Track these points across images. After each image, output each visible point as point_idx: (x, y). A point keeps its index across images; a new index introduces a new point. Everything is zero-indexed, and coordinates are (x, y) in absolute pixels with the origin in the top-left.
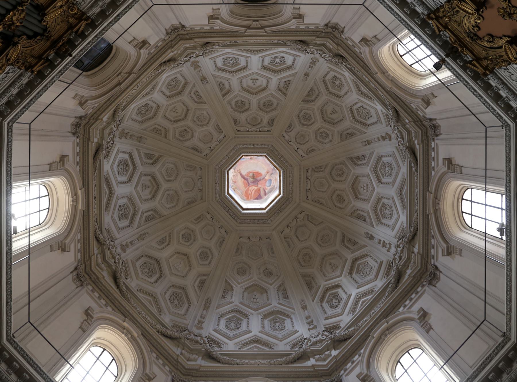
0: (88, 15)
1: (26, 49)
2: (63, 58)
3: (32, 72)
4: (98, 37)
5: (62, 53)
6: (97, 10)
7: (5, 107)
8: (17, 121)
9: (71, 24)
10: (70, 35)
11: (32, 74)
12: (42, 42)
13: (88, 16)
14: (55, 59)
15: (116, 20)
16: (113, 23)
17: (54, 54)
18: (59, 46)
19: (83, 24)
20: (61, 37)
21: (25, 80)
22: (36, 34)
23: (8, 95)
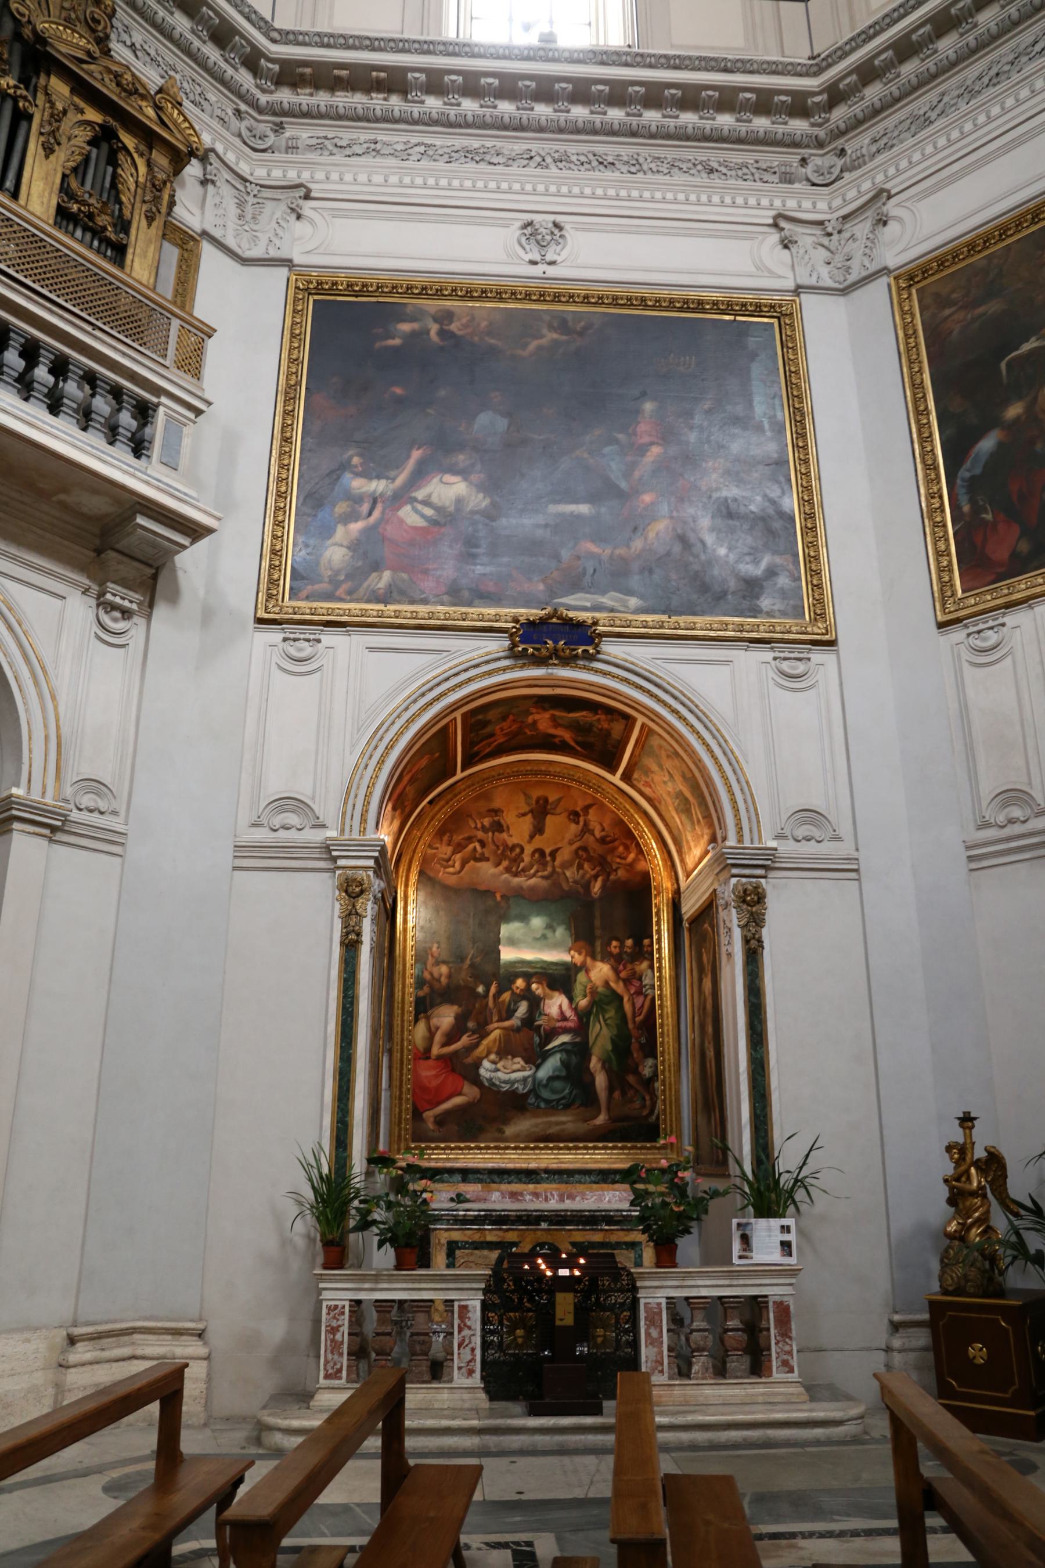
7: (231, 51)
8: (269, 18)
23: (197, 43)
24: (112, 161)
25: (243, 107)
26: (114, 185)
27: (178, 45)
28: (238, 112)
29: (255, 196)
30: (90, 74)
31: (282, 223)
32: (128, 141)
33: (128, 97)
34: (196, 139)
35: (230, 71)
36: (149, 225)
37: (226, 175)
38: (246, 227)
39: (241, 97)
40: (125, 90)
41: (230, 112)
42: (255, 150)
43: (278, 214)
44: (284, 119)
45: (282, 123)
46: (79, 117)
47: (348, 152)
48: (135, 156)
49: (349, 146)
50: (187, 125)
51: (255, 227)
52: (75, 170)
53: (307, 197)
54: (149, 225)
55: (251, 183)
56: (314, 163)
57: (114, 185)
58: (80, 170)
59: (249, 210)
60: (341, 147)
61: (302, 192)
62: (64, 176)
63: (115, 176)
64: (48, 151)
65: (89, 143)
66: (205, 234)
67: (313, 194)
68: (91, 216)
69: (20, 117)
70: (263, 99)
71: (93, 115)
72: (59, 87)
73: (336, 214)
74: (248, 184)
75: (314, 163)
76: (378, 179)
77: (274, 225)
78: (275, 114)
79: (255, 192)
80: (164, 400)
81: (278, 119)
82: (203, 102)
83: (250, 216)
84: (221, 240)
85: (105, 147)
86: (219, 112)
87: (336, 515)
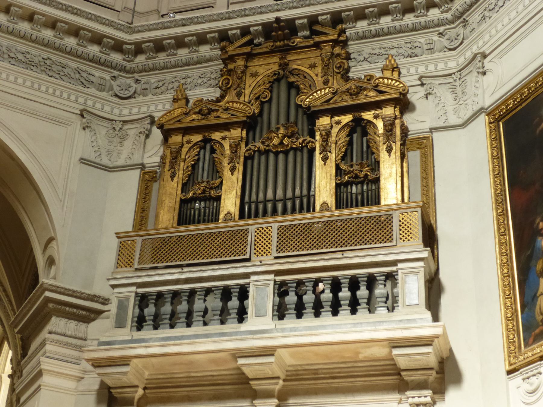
0: (220, 53)
1: (315, 78)
2: (291, 22)
3: (343, 31)
4: (227, 15)
5: (287, 31)
6: (205, 50)
7: (417, 10)
9: (247, 61)
10: (260, 44)
11: (345, 29)
12: (295, 66)
13: (221, 51)
14: (303, 27)
15: (189, 21)
16: (196, 20)
17: (299, 34)
18: (282, 42)
19: (231, 50)
20: (271, 52)
21: (362, 25)
22: (291, 86)
24: (365, 133)
25: (441, 29)
26: (368, 147)
27: (389, 33)
28: (441, 34)
29: (460, 79)
30: (336, 102)
31: (477, 85)
32: (368, 115)
33: (357, 97)
34: (401, 85)
35: (422, 20)
36: (390, 155)
37: (437, 81)
38: (461, 102)
39: (438, 25)
40: (354, 95)
41: (436, 38)
42: (454, 49)
43: (474, 79)
44: (464, 17)
45: (464, 19)
46: (340, 126)
47: (497, 9)
48: (374, 121)
49: (496, 5)
50: (394, 82)
51: (464, 99)
52: (343, 158)
53: (485, 56)
54: (390, 155)
55: (454, 73)
56: (482, 33)
57: (368, 147)
58: (345, 156)
59: (459, 90)
60: (493, 9)
61: (479, 57)
62: (338, 167)
63: (368, 141)
64: (325, 159)
65: (348, 136)
66: (432, 130)
67: (487, 52)
68: (357, 176)
69: (312, 152)
70: (449, 15)
71: (347, 119)
72: (324, 121)
73: (501, 56)
74: (453, 76)
75: (482, 33)
76: (513, 14)
77: (474, 88)
78: (459, 18)
79: (459, 77)
80: (400, 265)
81: (462, 19)
82: (413, 51)
83: (461, 93)
84: (446, 124)
85: (359, 129)
86: (426, 47)
87: (539, 272)
